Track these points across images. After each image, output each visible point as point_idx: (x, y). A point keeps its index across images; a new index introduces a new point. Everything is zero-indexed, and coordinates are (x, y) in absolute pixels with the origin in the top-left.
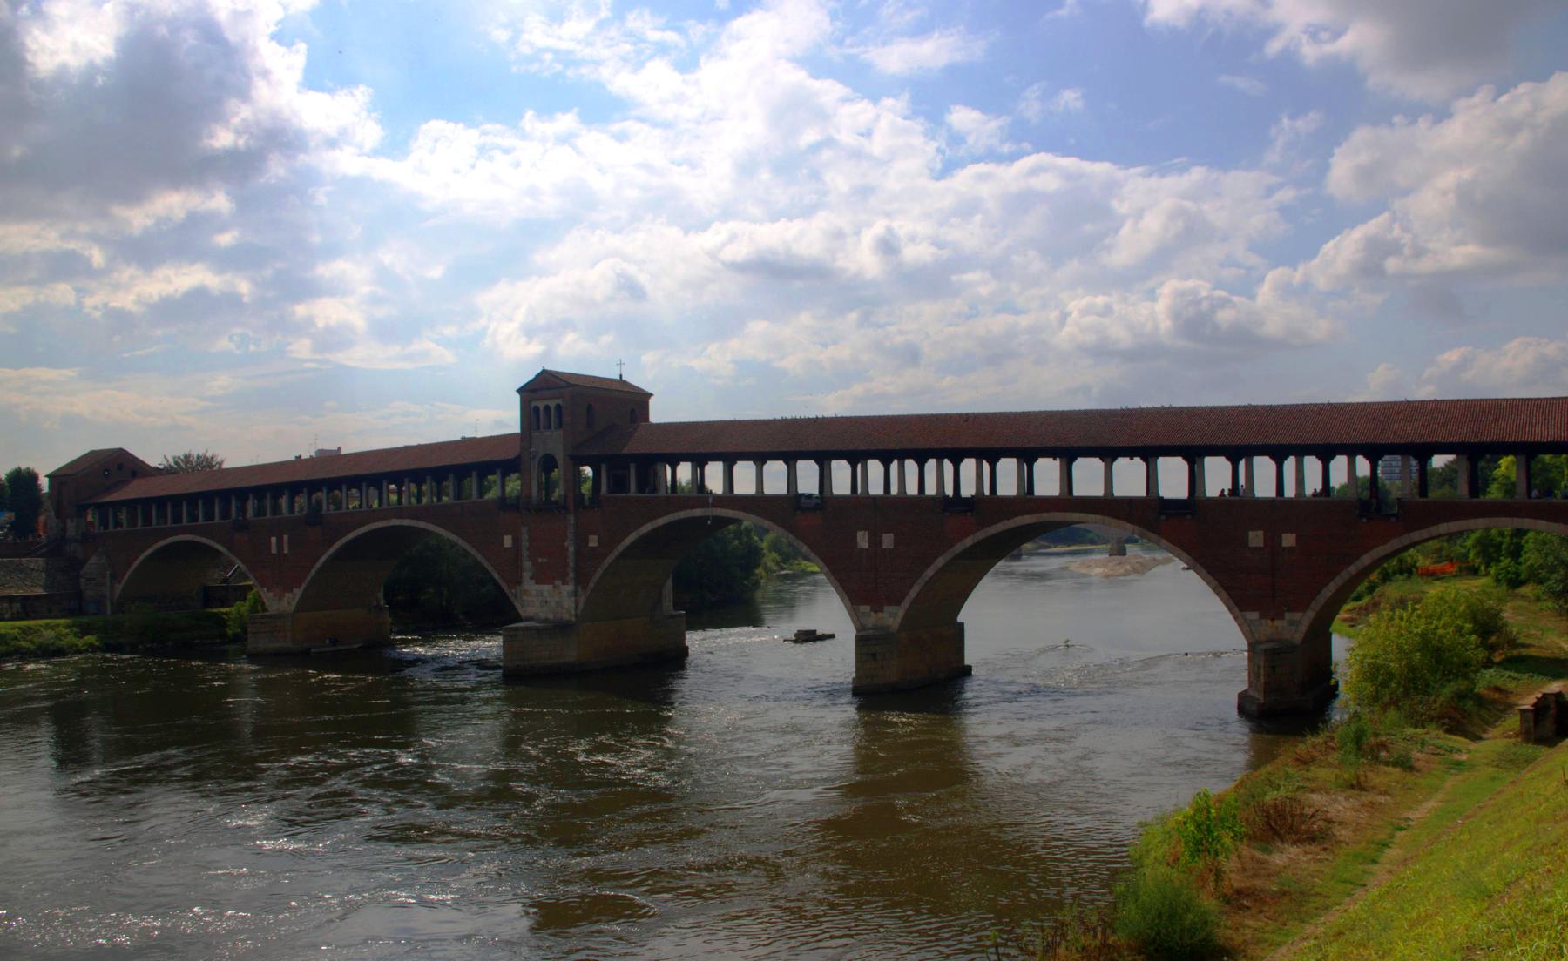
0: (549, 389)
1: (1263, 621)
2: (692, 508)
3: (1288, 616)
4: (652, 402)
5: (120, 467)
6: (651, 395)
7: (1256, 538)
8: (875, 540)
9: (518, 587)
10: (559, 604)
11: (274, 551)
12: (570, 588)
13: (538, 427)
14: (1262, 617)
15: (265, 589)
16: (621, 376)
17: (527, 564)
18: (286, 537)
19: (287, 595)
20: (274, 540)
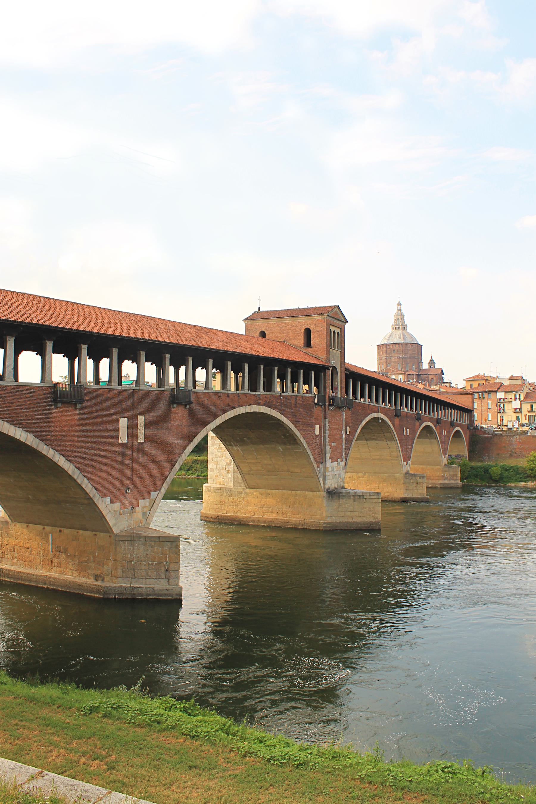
0: (339, 320)
2: (374, 412)
9: (321, 466)
10: (339, 474)
11: (123, 438)
12: (343, 463)
13: (330, 345)
15: (108, 499)
16: (259, 308)
17: (328, 447)
18: (141, 419)
19: (141, 502)
20: (123, 422)
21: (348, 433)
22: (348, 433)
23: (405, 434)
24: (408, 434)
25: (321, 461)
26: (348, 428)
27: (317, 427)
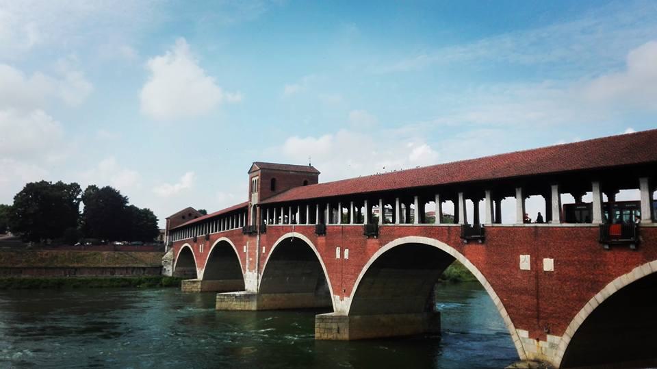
1: (531, 340)
2: (289, 232)
3: (549, 337)
4: (320, 176)
5: (190, 215)
6: (320, 173)
7: (525, 262)
8: (342, 254)
12: (256, 274)
14: (530, 336)
17: (247, 261)
21: (264, 251)
22: (264, 251)
23: (338, 256)
24: (346, 256)
25: (245, 270)
26: (264, 248)
27: (245, 247)
